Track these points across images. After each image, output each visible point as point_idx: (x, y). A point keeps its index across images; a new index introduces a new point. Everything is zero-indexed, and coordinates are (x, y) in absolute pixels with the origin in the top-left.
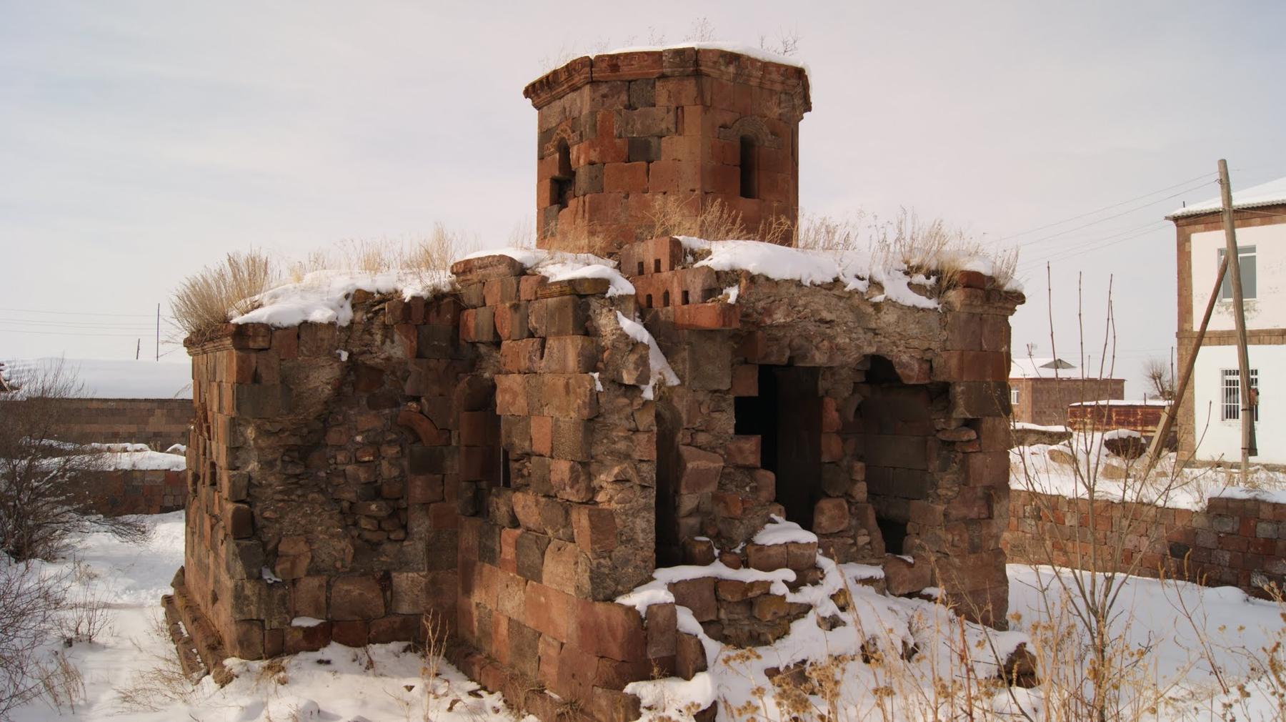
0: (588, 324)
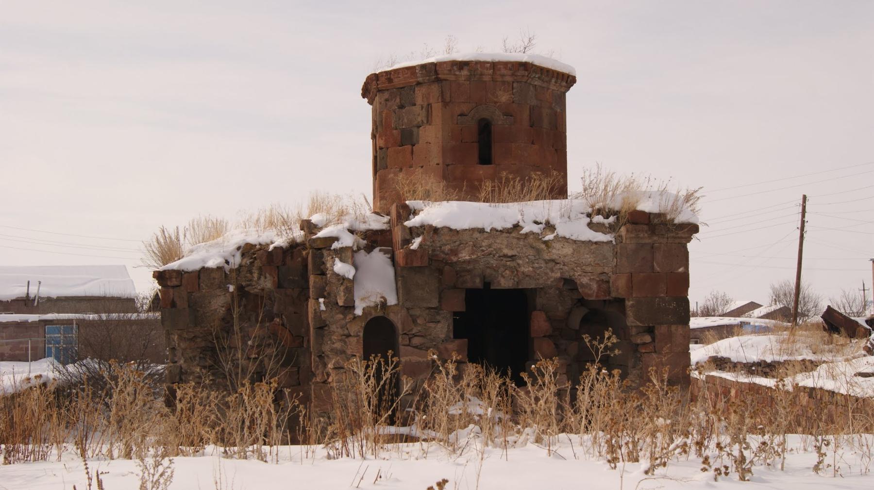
0: (322, 267)
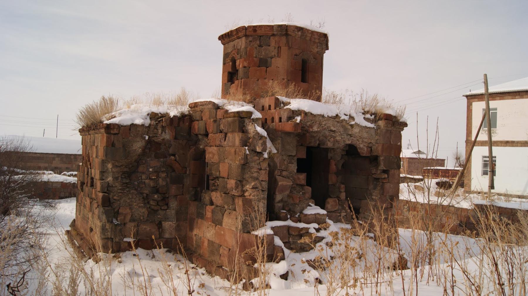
0: (244, 128)
